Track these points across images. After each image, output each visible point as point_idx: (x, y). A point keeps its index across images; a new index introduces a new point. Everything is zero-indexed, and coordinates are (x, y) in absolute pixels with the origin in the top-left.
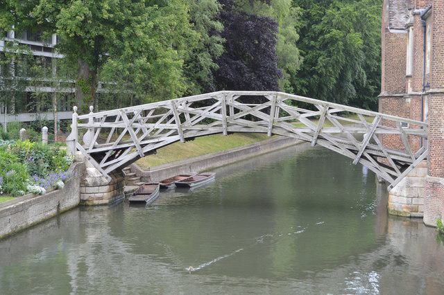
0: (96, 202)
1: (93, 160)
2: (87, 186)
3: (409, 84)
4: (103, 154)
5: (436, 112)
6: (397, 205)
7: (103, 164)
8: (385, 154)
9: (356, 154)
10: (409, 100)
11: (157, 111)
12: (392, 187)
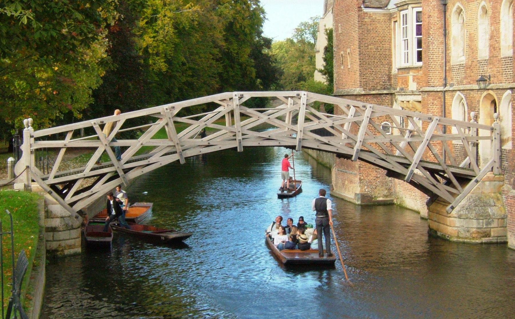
0: (66, 252)
1: (54, 193)
2: (54, 230)
3: (411, 78)
7: (69, 198)
8: (445, 167)
9: (407, 168)
10: (411, 98)
12: (453, 208)
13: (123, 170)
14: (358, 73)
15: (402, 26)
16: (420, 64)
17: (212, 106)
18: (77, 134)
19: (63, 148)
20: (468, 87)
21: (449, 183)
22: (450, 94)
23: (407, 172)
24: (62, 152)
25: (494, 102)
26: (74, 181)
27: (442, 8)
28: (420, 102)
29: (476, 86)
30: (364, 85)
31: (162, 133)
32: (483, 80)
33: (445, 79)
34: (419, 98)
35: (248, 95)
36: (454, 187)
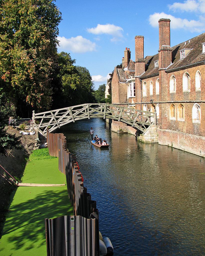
3: (132, 100)
4: (45, 127)
5: (164, 109)
6: (147, 140)
10: (132, 105)
11: (60, 112)
12: (144, 134)
13: (59, 124)
14: (118, 99)
15: (130, 87)
16: (135, 96)
17: (81, 107)
18: (47, 115)
19: (42, 118)
20: (148, 102)
21: (143, 127)
22: (143, 104)
23: (133, 125)
24: (42, 119)
25: (154, 106)
26: (45, 127)
27: (140, 82)
28: (135, 106)
29: (150, 102)
30: (120, 102)
31: (68, 115)
32: (151, 101)
33: (141, 100)
34: (135, 105)
35: (91, 104)
36: (145, 128)
